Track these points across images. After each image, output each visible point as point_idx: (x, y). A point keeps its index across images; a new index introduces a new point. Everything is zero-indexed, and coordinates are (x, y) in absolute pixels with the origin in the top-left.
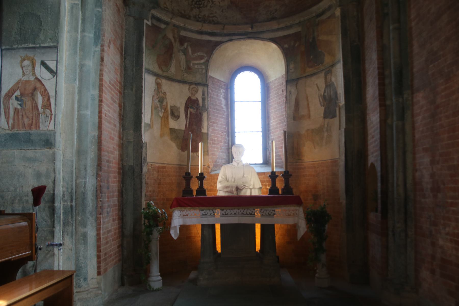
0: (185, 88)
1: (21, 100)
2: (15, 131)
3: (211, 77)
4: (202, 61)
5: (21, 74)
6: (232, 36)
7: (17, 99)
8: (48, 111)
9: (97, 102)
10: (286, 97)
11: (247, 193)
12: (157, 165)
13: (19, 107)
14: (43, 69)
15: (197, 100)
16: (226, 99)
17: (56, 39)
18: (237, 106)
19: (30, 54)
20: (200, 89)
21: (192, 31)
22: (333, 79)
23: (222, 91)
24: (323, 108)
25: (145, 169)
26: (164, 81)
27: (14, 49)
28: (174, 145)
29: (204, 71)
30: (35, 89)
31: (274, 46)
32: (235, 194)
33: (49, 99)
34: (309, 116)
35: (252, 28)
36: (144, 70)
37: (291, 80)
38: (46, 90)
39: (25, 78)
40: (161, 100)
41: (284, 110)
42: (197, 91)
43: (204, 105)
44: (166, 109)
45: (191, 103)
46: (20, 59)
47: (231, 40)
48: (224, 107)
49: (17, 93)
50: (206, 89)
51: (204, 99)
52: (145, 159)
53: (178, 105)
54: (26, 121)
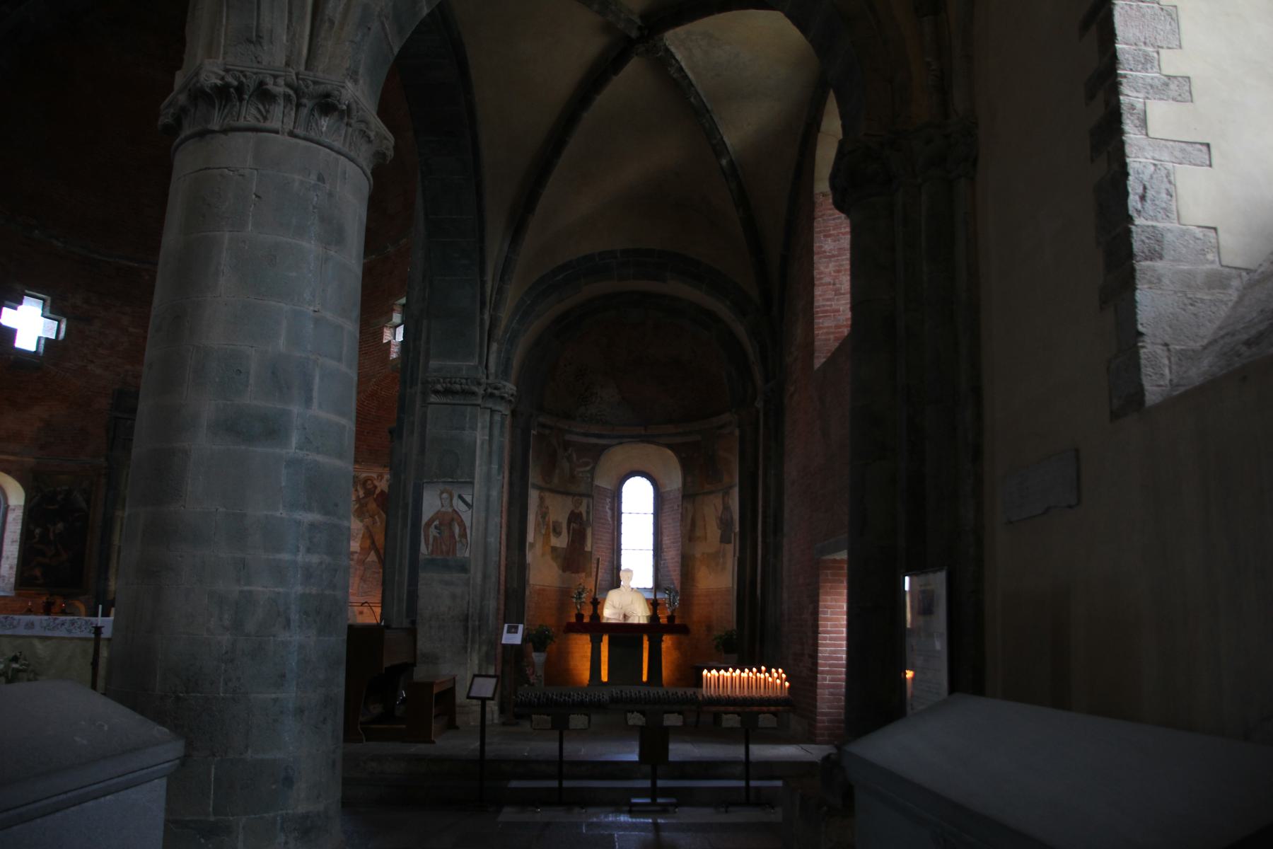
7: (436, 527)
11: (635, 620)
14: (460, 502)
16: (612, 509)
18: (624, 518)
19: (448, 487)
20: (585, 501)
21: (577, 434)
23: (608, 500)
25: (527, 593)
26: (547, 494)
28: (554, 564)
30: (452, 520)
31: (670, 452)
34: (706, 538)
37: (689, 495)
40: (543, 517)
43: (588, 520)
44: (548, 525)
45: (574, 517)
49: (436, 523)
51: (588, 513)
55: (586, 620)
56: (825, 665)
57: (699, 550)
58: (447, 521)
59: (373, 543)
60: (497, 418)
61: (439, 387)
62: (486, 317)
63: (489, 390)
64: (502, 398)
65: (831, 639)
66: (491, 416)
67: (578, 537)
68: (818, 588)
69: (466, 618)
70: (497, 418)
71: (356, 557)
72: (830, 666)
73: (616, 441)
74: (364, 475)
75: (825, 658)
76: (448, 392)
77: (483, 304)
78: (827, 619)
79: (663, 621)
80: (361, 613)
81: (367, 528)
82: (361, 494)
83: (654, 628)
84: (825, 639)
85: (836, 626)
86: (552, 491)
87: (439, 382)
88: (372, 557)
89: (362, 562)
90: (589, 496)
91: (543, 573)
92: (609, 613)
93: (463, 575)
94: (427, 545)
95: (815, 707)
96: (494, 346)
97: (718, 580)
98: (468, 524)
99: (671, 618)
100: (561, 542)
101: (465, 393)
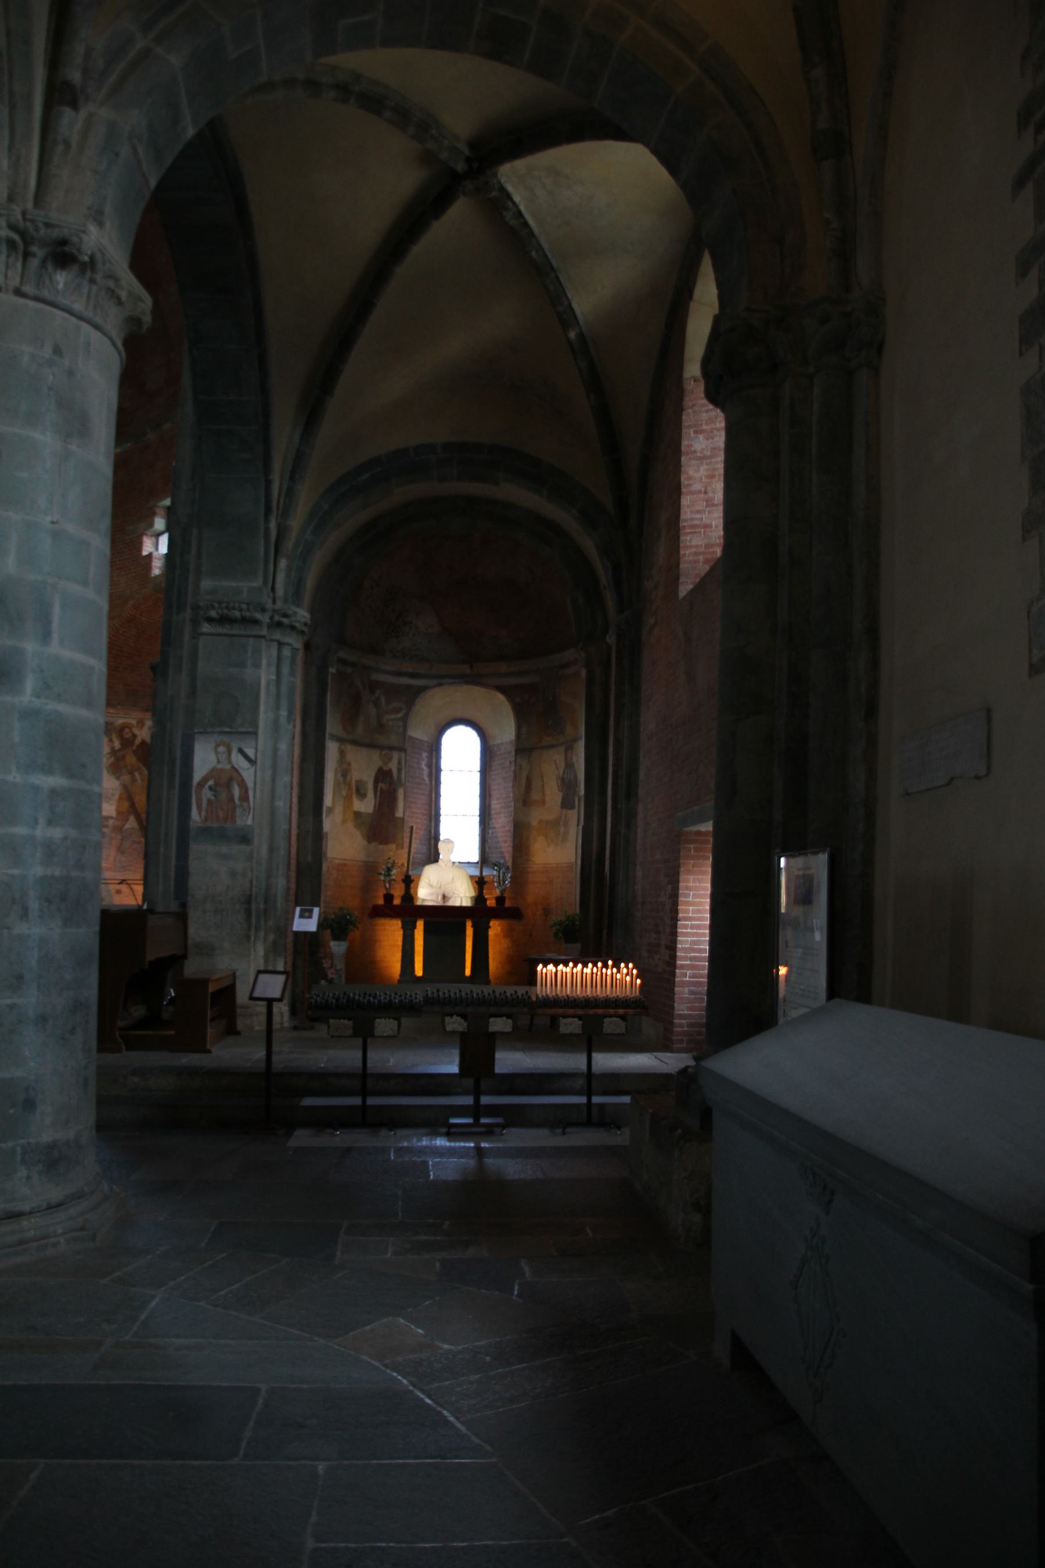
0: (375, 756)
1: (215, 791)
2: (208, 824)
3: (411, 738)
4: (400, 715)
5: (215, 761)
6: (442, 679)
7: (211, 788)
8: (245, 804)
9: (289, 789)
10: (515, 772)
12: (337, 861)
13: (213, 798)
14: (241, 757)
15: (390, 771)
16: (430, 766)
17: (255, 725)
18: (444, 777)
19: (226, 739)
20: (395, 755)
21: (387, 672)
22: (574, 759)
23: (425, 755)
24: (561, 794)
26: (349, 747)
27: (208, 733)
29: (401, 730)
30: (231, 779)
31: (501, 697)
32: (441, 904)
33: (246, 791)
34: (544, 803)
35: (471, 668)
36: (327, 736)
37: (523, 749)
38: (243, 780)
39: (220, 766)
41: (510, 789)
42: (390, 759)
44: (350, 785)
45: (382, 775)
46: (213, 745)
47: (440, 685)
48: (426, 778)
49: (211, 783)
50: (403, 755)
51: (399, 770)
52: (325, 853)
53: (365, 779)
54: (221, 814)
55: (397, 901)
56: (685, 958)
57: (536, 816)
58: (225, 780)
59: (133, 805)
60: (287, 652)
61: (213, 614)
62: (273, 525)
63: (277, 618)
64: (293, 628)
65: (692, 927)
66: (279, 650)
67: (387, 800)
68: (678, 866)
69: (249, 900)
70: (287, 652)
71: (111, 822)
72: (692, 959)
73: (435, 682)
74: (120, 721)
75: (685, 950)
76: (224, 620)
77: (268, 510)
78: (688, 903)
79: (491, 903)
80: (119, 892)
81: (125, 787)
82: (117, 744)
83: (479, 912)
84: (686, 927)
85: (699, 911)
86: (355, 743)
87: (213, 607)
88: (132, 823)
89: (119, 829)
90: (402, 749)
91: (344, 844)
92: (426, 893)
93: (244, 848)
94: (199, 808)
95: (673, 1008)
96: (283, 563)
97: (558, 854)
98: (250, 784)
99: (500, 900)
100: (366, 806)
101: (246, 621)
